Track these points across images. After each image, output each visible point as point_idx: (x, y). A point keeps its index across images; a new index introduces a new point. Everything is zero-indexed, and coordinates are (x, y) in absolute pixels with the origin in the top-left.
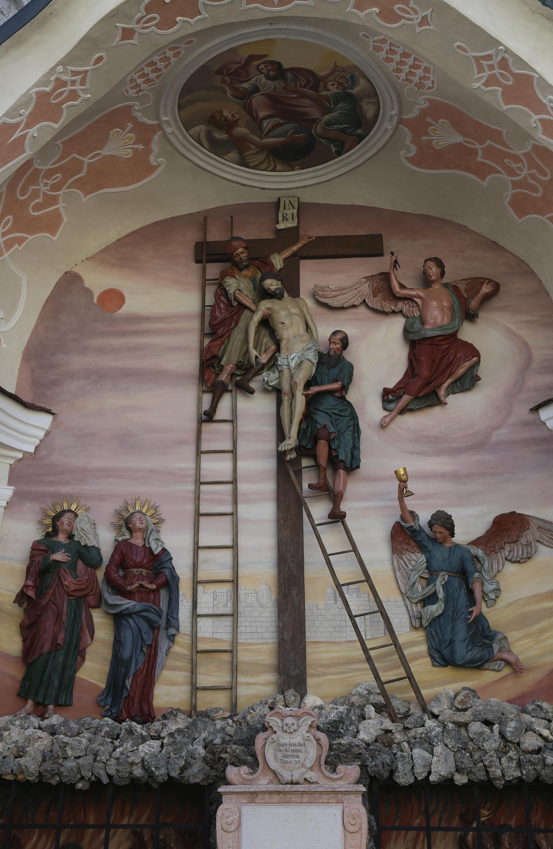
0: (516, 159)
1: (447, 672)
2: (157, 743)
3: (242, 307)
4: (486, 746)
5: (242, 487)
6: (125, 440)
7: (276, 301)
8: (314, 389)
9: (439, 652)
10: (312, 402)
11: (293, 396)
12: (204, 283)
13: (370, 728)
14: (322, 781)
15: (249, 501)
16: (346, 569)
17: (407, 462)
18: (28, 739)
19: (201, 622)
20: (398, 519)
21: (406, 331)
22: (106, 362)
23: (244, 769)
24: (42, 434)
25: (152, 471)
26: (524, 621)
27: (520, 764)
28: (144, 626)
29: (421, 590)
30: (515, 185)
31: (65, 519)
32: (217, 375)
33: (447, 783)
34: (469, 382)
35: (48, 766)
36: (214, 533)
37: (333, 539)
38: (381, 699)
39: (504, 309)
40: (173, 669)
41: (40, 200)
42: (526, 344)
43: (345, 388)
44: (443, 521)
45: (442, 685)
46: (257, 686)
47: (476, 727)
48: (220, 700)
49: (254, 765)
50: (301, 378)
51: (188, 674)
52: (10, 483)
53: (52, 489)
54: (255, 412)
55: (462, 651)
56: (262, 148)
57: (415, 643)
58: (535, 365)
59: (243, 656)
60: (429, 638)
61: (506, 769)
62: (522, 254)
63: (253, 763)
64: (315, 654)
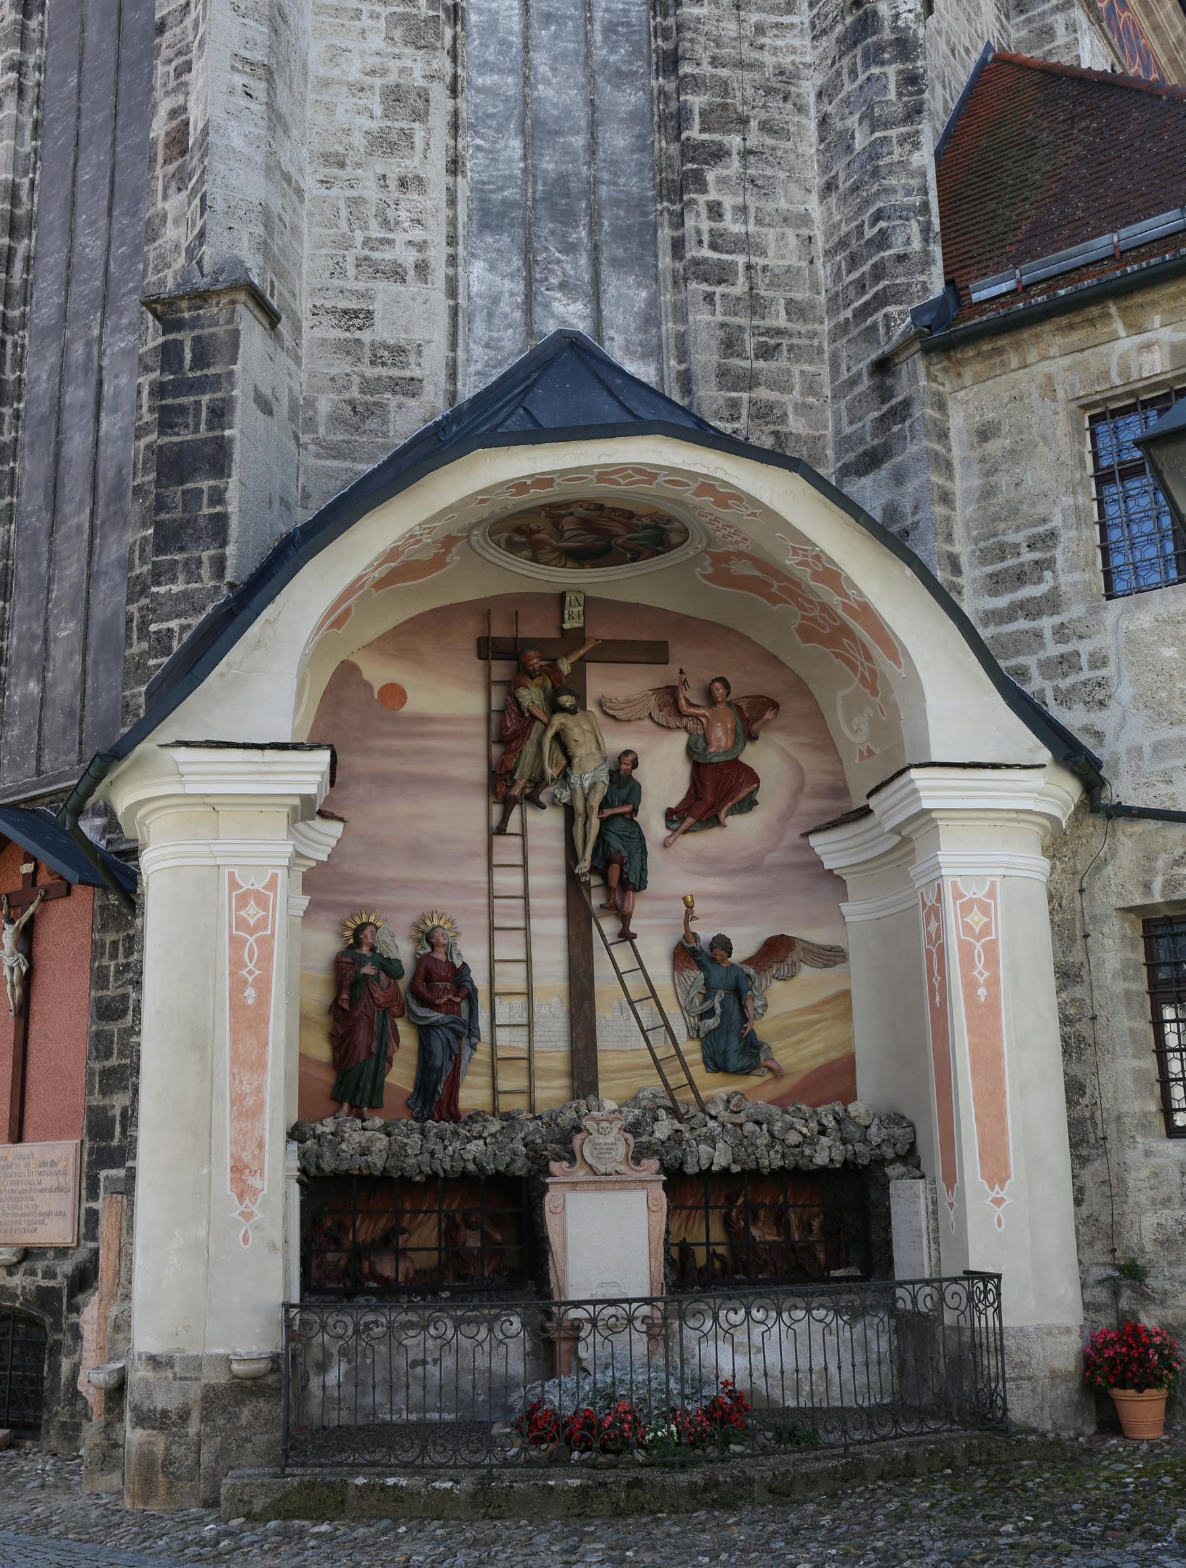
1: (719, 1077)
2: (481, 1142)
3: (533, 718)
4: (759, 1142)
5: (533, 902)
6: (417, 851)
8: (608, 812)
9: (712, 1059)
10: (604, 822)
11: (587, 818)
12: (489, 684)
13: (663, 1128)
14: (629, 1172)
16: (635, 984)
17: (692, 884)
18: (369, 1140)
19: (500, 1032)
21: (690, 750)
22: (391, 765)
23: (565, 1164)
24: (334, 843)
26: (786, 1032)
27: (783, 1156)
28: (451, 1036)
30: (803, 617)
31: (368, 931)
32: (510, 788)
33: (726, 1171)
34: (748, 804)
35: (392, 1162)
37: (622, 953)
38: (669, 1103)
39: (781, 729)
40: (474, 1074)
42: (800, 767)
43: (635, 811)
44: (722, 944)
46: (552, 1090)
47: (750, 1127)
48: (520, 1102)
49: (572, 1160)
50: (596, 800)
51: (489, 1079)
52: (304, 892)
53: (347, 898)
54: (544, 825)
55: (734, 1060)
56: (556, 549)
57: (693, 1051)
58: (807, 789)
59: (538, 1063)
60: (704, 1047)
61: (773, 1160)
62: (800, 672)
64: (605, 1061)
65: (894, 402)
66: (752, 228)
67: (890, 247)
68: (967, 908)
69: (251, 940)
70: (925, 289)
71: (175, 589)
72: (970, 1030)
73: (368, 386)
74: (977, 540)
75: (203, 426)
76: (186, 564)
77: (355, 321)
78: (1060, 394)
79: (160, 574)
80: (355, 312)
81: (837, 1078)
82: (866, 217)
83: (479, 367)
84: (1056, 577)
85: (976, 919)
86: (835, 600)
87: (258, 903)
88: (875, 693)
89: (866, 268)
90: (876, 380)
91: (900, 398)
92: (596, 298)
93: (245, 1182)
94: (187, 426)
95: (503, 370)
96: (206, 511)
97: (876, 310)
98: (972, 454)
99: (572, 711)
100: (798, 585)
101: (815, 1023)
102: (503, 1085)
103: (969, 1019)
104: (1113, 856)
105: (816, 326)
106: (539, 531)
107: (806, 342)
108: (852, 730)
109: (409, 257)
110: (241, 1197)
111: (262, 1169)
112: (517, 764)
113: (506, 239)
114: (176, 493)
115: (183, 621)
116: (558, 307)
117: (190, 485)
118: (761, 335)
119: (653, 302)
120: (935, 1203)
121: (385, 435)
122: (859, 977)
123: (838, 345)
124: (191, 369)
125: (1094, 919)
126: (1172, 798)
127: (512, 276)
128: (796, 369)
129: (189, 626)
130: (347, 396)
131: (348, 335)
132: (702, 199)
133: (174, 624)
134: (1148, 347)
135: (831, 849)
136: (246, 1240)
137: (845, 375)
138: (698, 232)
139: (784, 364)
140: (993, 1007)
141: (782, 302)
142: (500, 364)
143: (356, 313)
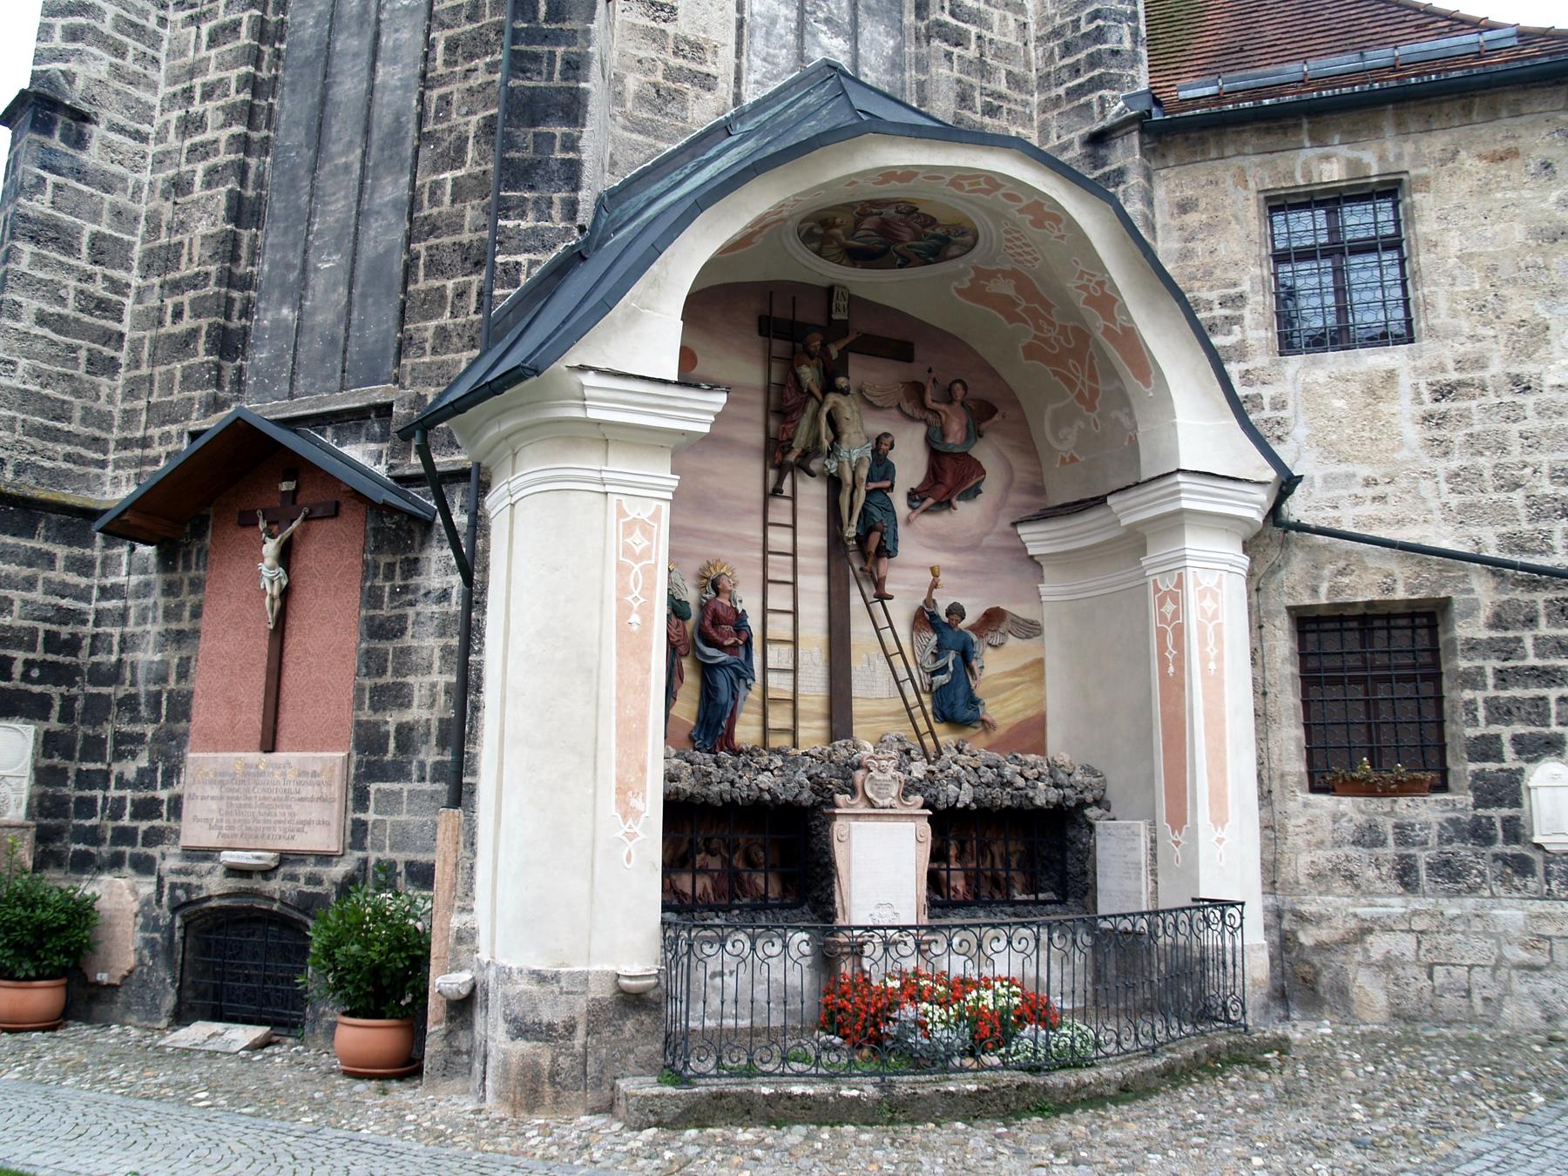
0: (1051, 324)
3: (811, 394)
5: (799, 559)
8: (872, 485)
10: (868, 493)
11: (854, 487)
12: (769, 359)
13: (919, 769)
15: (806, 573)
18: (676, 767)
20: (920, 602)
21: (928, 440)
25: (727, 535)
29: (930, 665)
32: (785, 454)
33: (967, 806)
36: (779, 598)
40: (747, 712)
44: (956, 611)
45: (946, 737)
46: (813, 732)
50: (864, 472)
56: (841, 245)
59: (801, 705)
61: (1004, 798)
63: (852, 790)
64: (858, 707)
65: (1107, 169)
68: (1202, 596)
69: (637, 567)
70: (1134, 81)
71: (524, 225)
72: (1204, 697)
73: (671, 74)
75: (557, 75)
76: (536, 202)
77: (663, 14)
78: (1252, 184)
79: (508, 209)
81: (1032, 733)
82: (1083, 15)
83: (757, 76)
84: (1243, 332)
85: (1208, 603)
86: (1098, 324)
87: (643, 533)
88: (1091, 408)
89: (1082, 55)
90: (1088, 150)
91: (1114, 167)
92: (854, 37)
93: (627, 804)
94: (540, 73)
95: (779, 84)
96: (559, 155)
97: (1091, 91)
99: (845, 392)
100: (1048, 306)
101: (1017, 684)
102: (772, 723)
103: (1204, 687)
104: (1287, 563)
106: (838, 226)
107: (1020, 108)
108: (1060, 441)
110: (625, 817)
111: (644, 791)
112: (794, 434)
114: (526, 135)
115: (532, 256)
116: (824, 39)
119: (898, 50)
120: (1154, 841)
121: (684, 120)
122: (1052, 647)
124: (546, 21)
125: (1268, 612)
126: (1338, 521)
129: (538, 262)
130: (652, 79)
131: (654, 24)
133: (523, 258)
134: (1327, 158)
135: (1038, 539)
136: (629, 860)
140: (1220, 683)
142: (775, 78)
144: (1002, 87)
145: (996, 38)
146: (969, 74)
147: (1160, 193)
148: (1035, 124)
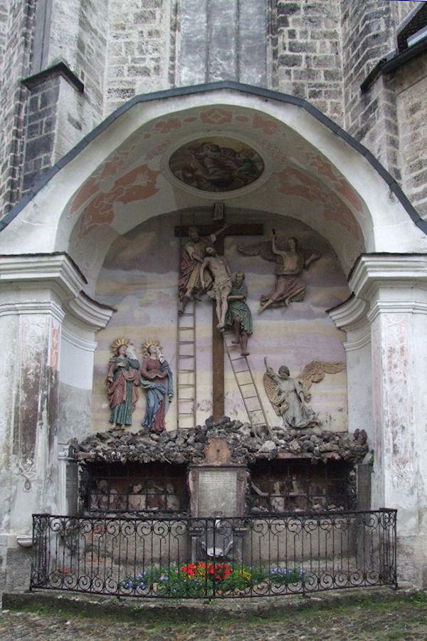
7: (213, 258)
10: (230, 302)
11: (221, 303)
41: (104, 207)
56: (208, 181)
66: (309, 40)
67: (370, 32)
74: (409, 162)
77: (127, 94)
80: (127, 90)
82: (360, 23)
89: (360, 46)
91: (373, 101)
96: (43, 167)
97: (364, 64)
98: (408, 121)
105: (339, 81)
107: (334, 89)
109: (151, 65)
113: (197, 57)
114: (32, 162)
117: (37, 158)
118: (313, 87)
123: (348, 88)
124: (41, 108)
127: (200, 72)
128: (328, 102)
131: (123, 100)
132: (286, 29)
137: (351, 100)
138: (284, 44)
139: (323, 99)
141: (323, 72)
143: (127, 91)
144: (322, 80)
145: (317, 55)
146: (300, 78)
147: (402, 107)
148: (343, 95)
